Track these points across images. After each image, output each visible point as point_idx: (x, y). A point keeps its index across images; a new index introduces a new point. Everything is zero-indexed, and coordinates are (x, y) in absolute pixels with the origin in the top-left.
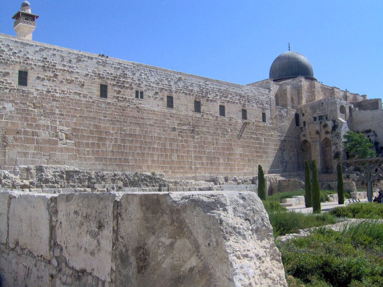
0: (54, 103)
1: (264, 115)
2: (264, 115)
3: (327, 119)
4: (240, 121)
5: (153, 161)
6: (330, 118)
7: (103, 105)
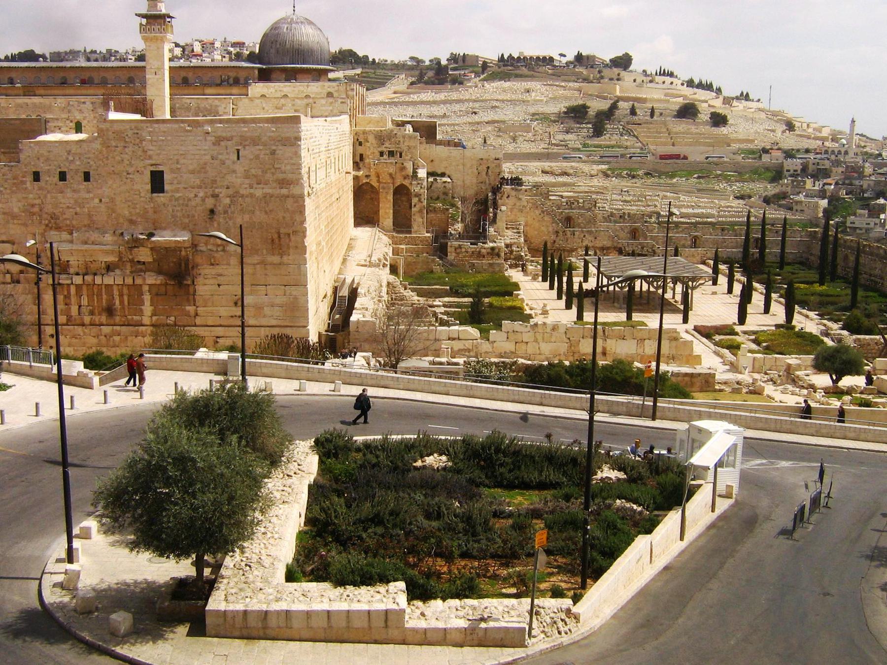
3: (401, 156)
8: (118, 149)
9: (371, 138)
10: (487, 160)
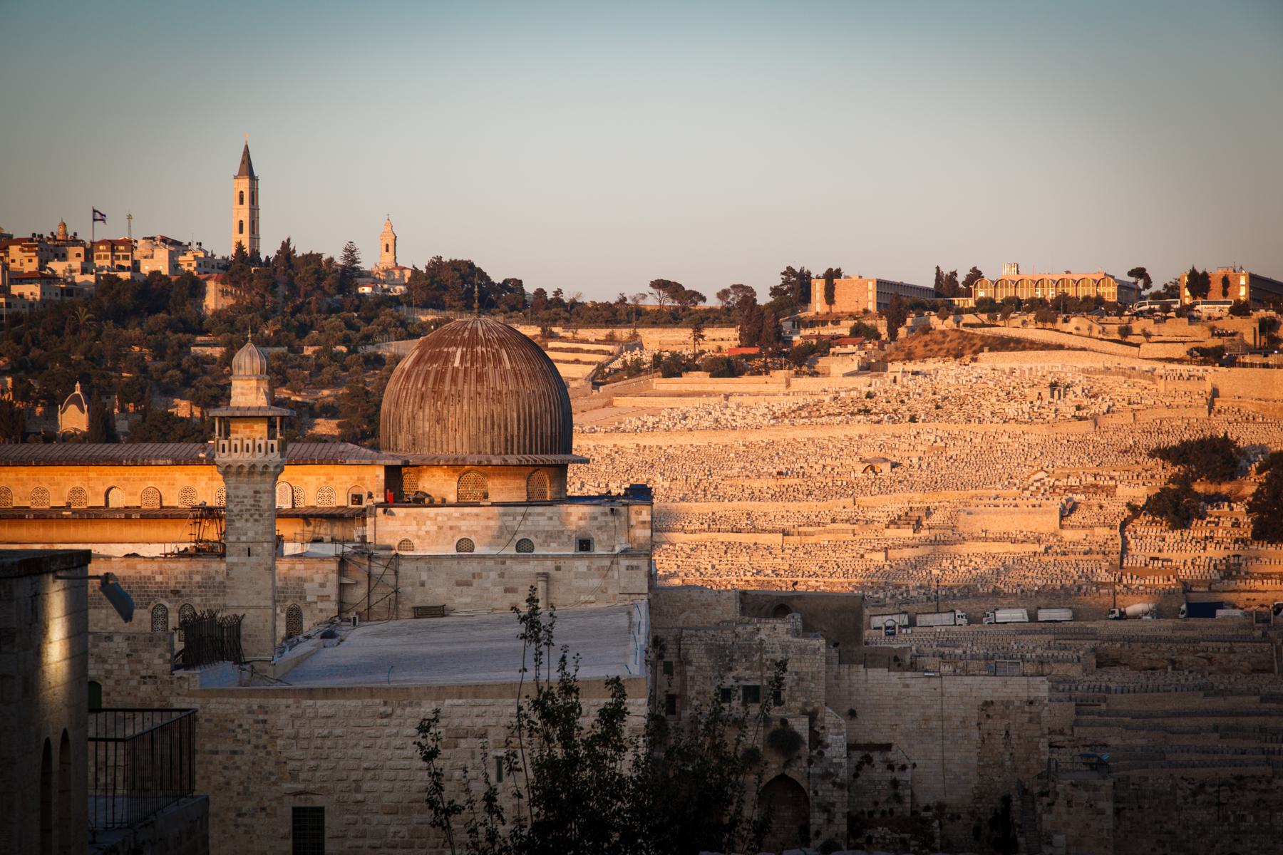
6: (793, 704)
8: (219, 757)
10: (1007, 704)
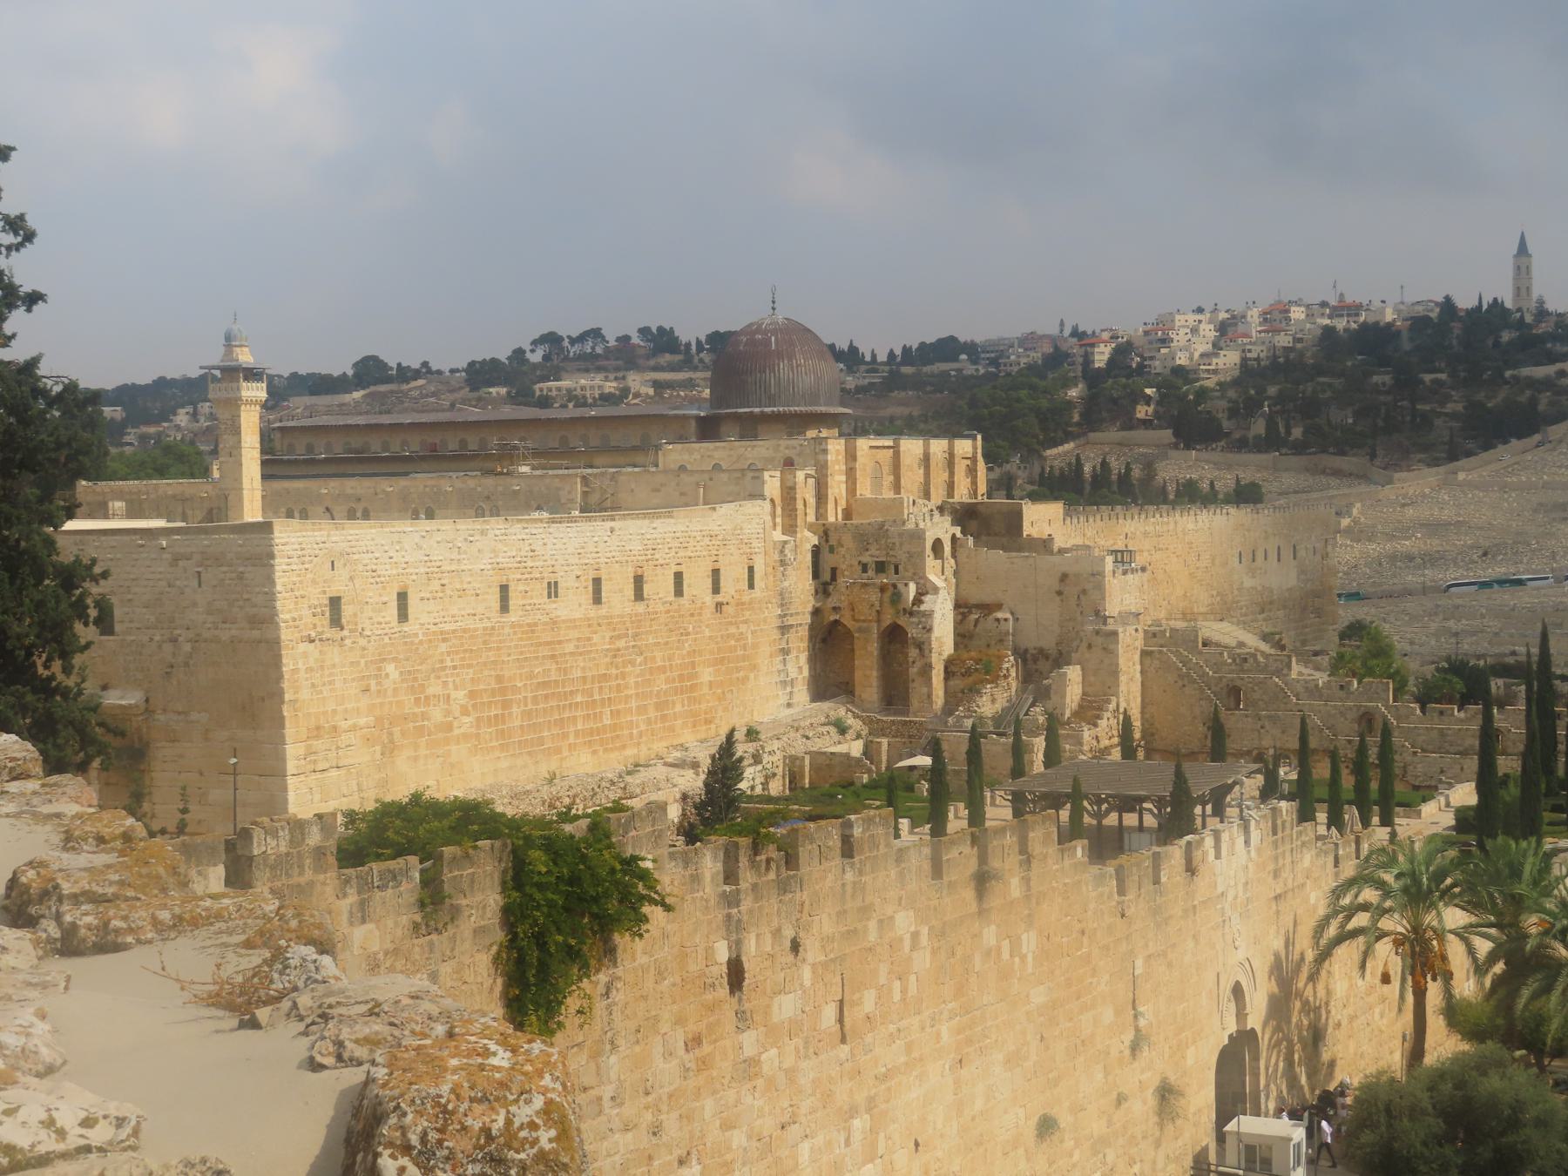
0: (443, 647)
1: (751, 569)
2: (751, 569)
3: (897, 572)
4: (709, 600)
5: (577, 733)
7: (507, 630)
9: (848, 541)
